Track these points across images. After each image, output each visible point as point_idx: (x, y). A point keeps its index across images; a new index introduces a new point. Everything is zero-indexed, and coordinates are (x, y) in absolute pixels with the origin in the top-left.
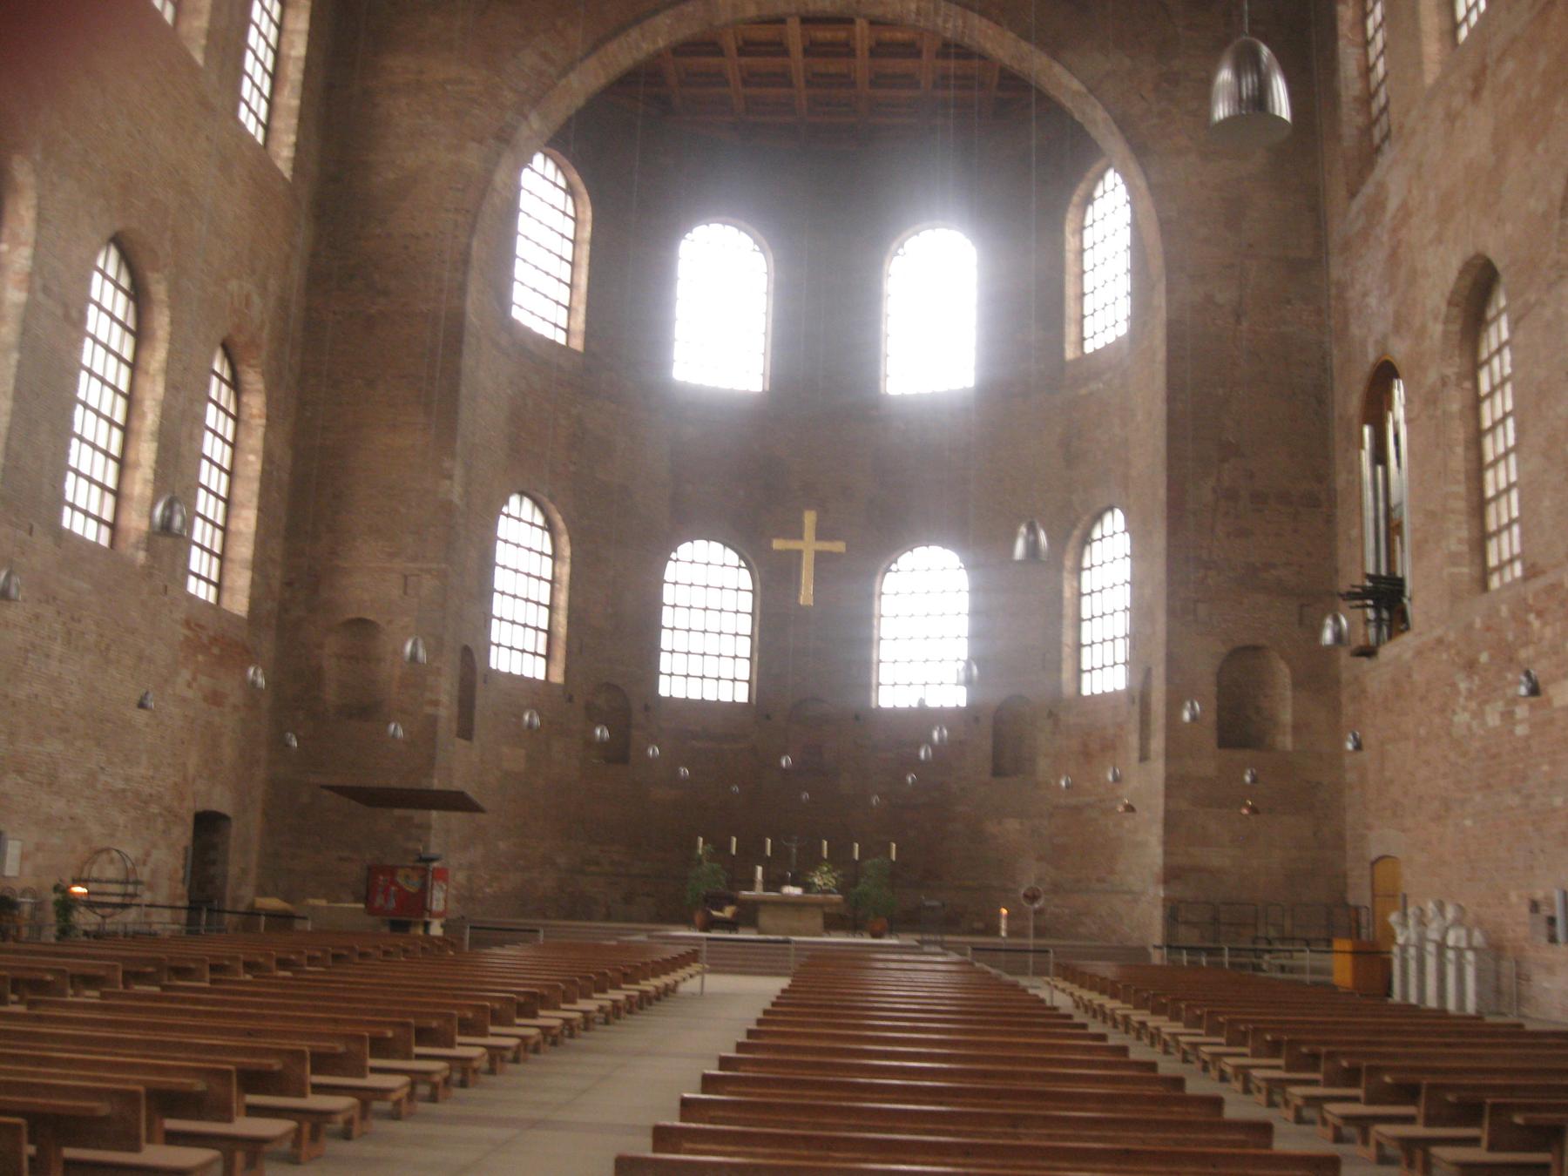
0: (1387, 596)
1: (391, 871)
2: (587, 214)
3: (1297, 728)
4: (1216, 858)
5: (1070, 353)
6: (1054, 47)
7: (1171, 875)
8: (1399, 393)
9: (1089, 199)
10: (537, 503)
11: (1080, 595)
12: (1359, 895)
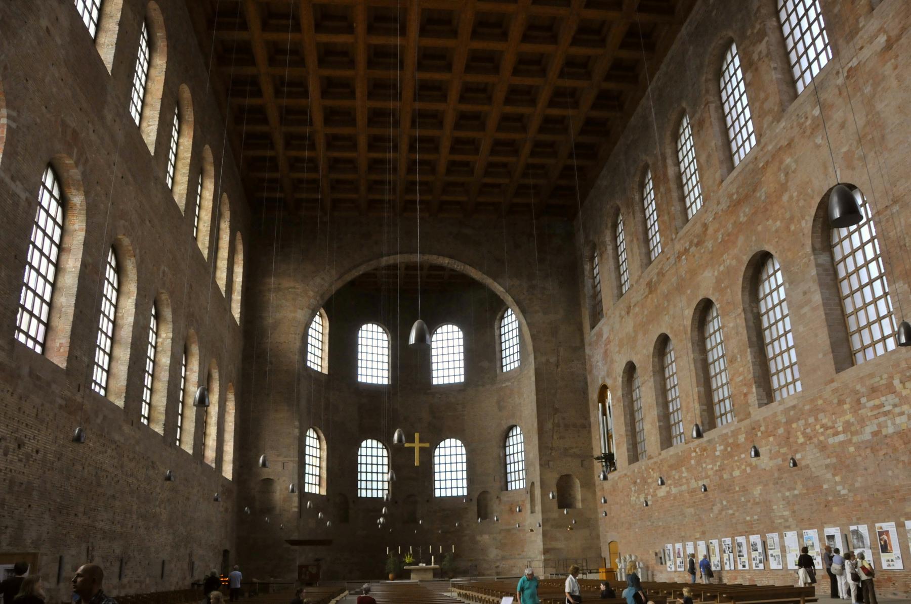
0: (609, 459)
1: (306, 567)
2: (327, 324)
3: (583, 501)
4: (560, 545)
5: (498, 371)
6: (495, 278)
7: (546, 551)
8: (609, 394)
9: (502, 318)
10: (314, 430)
11: (506, 456)
12: (605, 554)
